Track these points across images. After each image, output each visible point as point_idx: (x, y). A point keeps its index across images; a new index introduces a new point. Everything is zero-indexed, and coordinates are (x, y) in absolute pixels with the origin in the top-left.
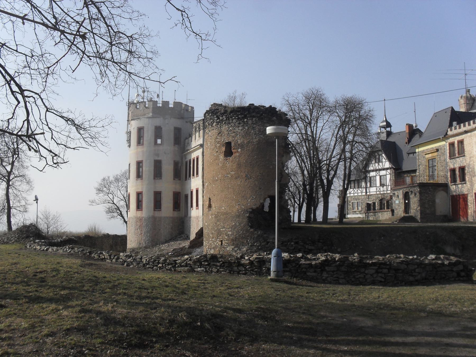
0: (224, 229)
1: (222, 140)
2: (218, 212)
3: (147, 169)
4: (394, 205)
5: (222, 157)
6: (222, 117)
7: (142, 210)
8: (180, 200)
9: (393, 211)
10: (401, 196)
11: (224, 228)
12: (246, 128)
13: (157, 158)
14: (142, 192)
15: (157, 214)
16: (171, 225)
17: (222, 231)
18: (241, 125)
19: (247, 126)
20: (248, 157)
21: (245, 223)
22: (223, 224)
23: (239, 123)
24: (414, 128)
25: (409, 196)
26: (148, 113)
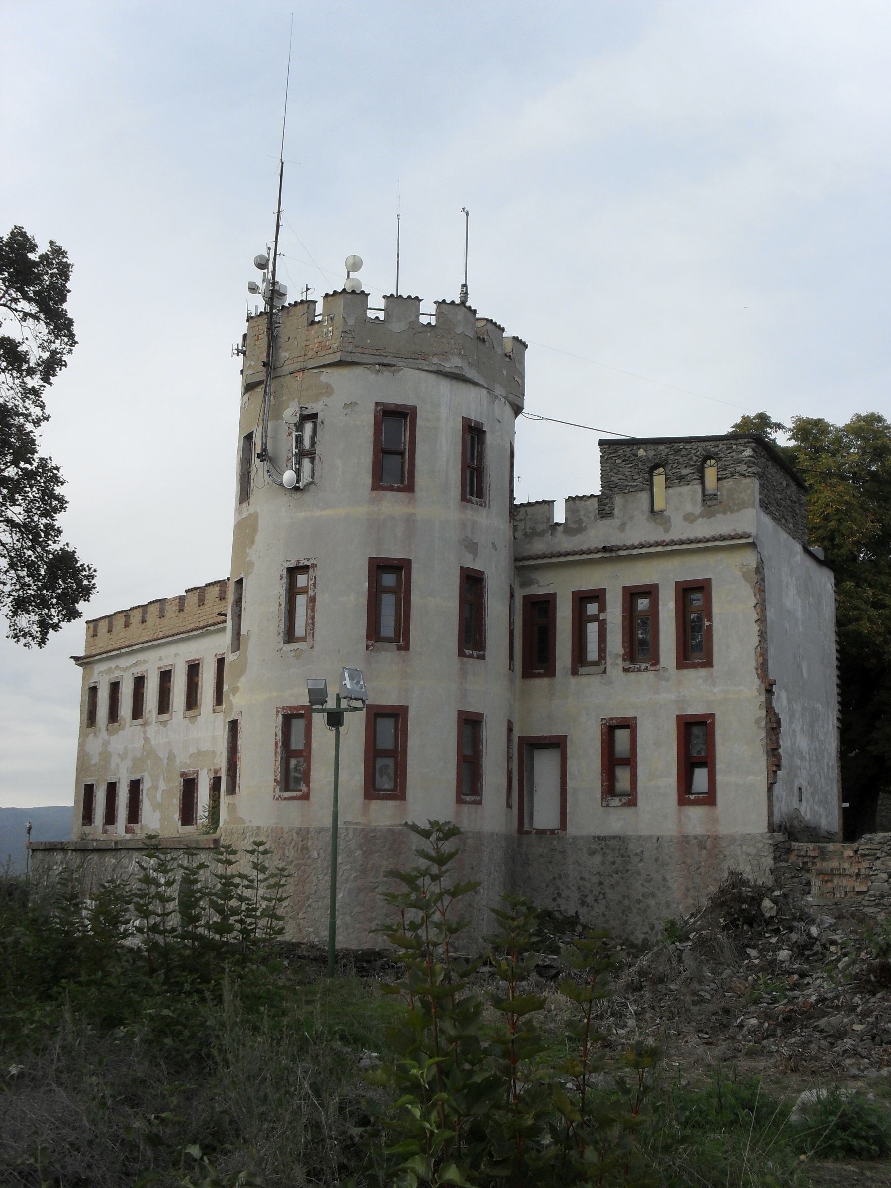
14: (405, 709)
16: (504, 868)
26: (444, 355)
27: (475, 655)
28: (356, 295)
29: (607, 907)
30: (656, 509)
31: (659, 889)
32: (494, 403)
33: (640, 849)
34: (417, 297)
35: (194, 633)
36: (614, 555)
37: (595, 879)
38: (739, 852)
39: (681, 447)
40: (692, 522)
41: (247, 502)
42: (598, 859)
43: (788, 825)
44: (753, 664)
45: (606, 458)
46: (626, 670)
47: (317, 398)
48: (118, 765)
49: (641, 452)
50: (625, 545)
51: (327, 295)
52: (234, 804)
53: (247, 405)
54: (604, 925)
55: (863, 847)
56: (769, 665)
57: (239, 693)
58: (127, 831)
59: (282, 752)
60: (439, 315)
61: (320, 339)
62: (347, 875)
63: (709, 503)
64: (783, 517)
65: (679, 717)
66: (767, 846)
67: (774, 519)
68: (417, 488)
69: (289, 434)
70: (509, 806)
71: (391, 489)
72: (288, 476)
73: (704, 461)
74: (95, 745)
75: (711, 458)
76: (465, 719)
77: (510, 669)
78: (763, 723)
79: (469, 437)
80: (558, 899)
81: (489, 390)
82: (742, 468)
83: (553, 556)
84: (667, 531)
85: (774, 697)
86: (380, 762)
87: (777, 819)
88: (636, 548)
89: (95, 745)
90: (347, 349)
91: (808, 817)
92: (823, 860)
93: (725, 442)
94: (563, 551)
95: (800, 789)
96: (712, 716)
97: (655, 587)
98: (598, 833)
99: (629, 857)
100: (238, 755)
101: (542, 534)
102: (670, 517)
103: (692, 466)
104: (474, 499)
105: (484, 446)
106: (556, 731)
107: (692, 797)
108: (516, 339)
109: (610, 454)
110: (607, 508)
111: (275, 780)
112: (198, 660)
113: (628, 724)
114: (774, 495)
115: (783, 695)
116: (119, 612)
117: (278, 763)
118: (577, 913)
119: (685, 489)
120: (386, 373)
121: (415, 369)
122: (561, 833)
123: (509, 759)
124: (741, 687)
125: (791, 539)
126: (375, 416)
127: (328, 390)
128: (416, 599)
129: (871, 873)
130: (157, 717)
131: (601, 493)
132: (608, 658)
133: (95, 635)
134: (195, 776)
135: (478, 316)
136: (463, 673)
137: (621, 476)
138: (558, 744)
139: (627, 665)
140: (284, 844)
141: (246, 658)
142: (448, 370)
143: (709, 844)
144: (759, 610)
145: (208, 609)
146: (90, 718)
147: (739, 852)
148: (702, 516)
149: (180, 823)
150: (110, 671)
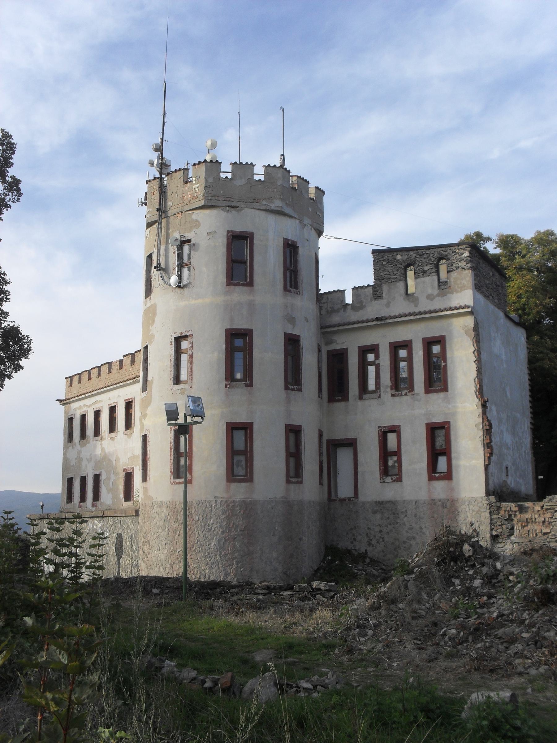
14: (251, 424)
16: (318, 523)
26: (270, 199)
27: (296, 389)
28: (213, 164)
29: (385, 547)
30: (409, 292)
31: (417, 534)
32: (303, 228)
33: (405, 509)
34: (252, 164)
35: (129, 382)
36: (383, 322)
37: (377, 529)
38: (467, 509)
39: (424, 253)
40: (432, 300)
41: (150, 297)
42: (378, 516)
43: (499, 491)
44: (473, 389)
45: (376, 261)
46: (393, 395)
47: (191, 229)
48: (86, 466)
49: (399, 257)
50: (390, 316)
51: (195, 165)
52: (146, 488)
53: (148, 236)
54: (383, 558)
55: (547, 504)
56: (484, 389)
57: (147, 418)
58: (93, 505)
59: (174, 454)
60: (266, 174)
61: (191, 192)
62: (217, 530)
63: (442, 287)
64: (491, 295)
65: (427, 424)
66: (485, 505)
67: (485, 296)
68: (255, 283)
69: (174, 253)
70: (321, 484)
71: (238, 285)
72: (174, 279)
73: (439, 261)
74: (72, 454)
75: (443, 258)
76: (290, 430)
77: (319, 397)
78: (481, 426)
79: (288, 251)
80: (354, 542)
81: (301, 221)
82: (463, 264)
83: (344, 324)
84: (416, 306)
85: (488, 409)
86: (236, 458)
87: (491, 487)
88: (397, 317)
89: (72, 454)
90: (208, 198)
91: (513, 485)
92: (521, 513)
93: (451, 248)
94: (351, 321)
95: (507, 468)
96: (448, 423)
97: (410, 342)
98: (378, 500)
99: (398, 514)
100: (148, 456)
101: (338, 311)
102: (418, 298)
103: (431, 264)
104: (292, 290)
105: (298, 256)
106: (350, 435)
107: (437, 475)
108: (317, 188)
109: (379, 258)
110: (378, 293)
111: (171, 472)
112: (131, 399)
113: (396, 430)
114: (484, 281)
115: (494, 408)
116: (85, 371)
117: (172, 461)
118: (366, 550)
119: (427, 279)
120: (234, 212)
121: (252, 208)
122: (355, 500)
123: (320, 454)
124: (466, 404)
125: (496, 309)
126: (227, 239)
127: (197, 224)
128: (256, 354)
129: (552, 521)
130: (108, 435)
131: (374, 284)
132: (381, 388)
133: (71, 385)
134: (131, 471)
135: (291, 174)
136: (288, 401)
137: (386, 273)
138: (352, 444)
139: (394, 392)
140: (177, 511)
141: (151, 396)
142: (273, 208)
143: (448, 504)
144: (476, 354)
145: (137, 367)
146: (70, 437)
147: (467, 509)
148: (438, 295)
149: (124, 500)
150: (80, 407)
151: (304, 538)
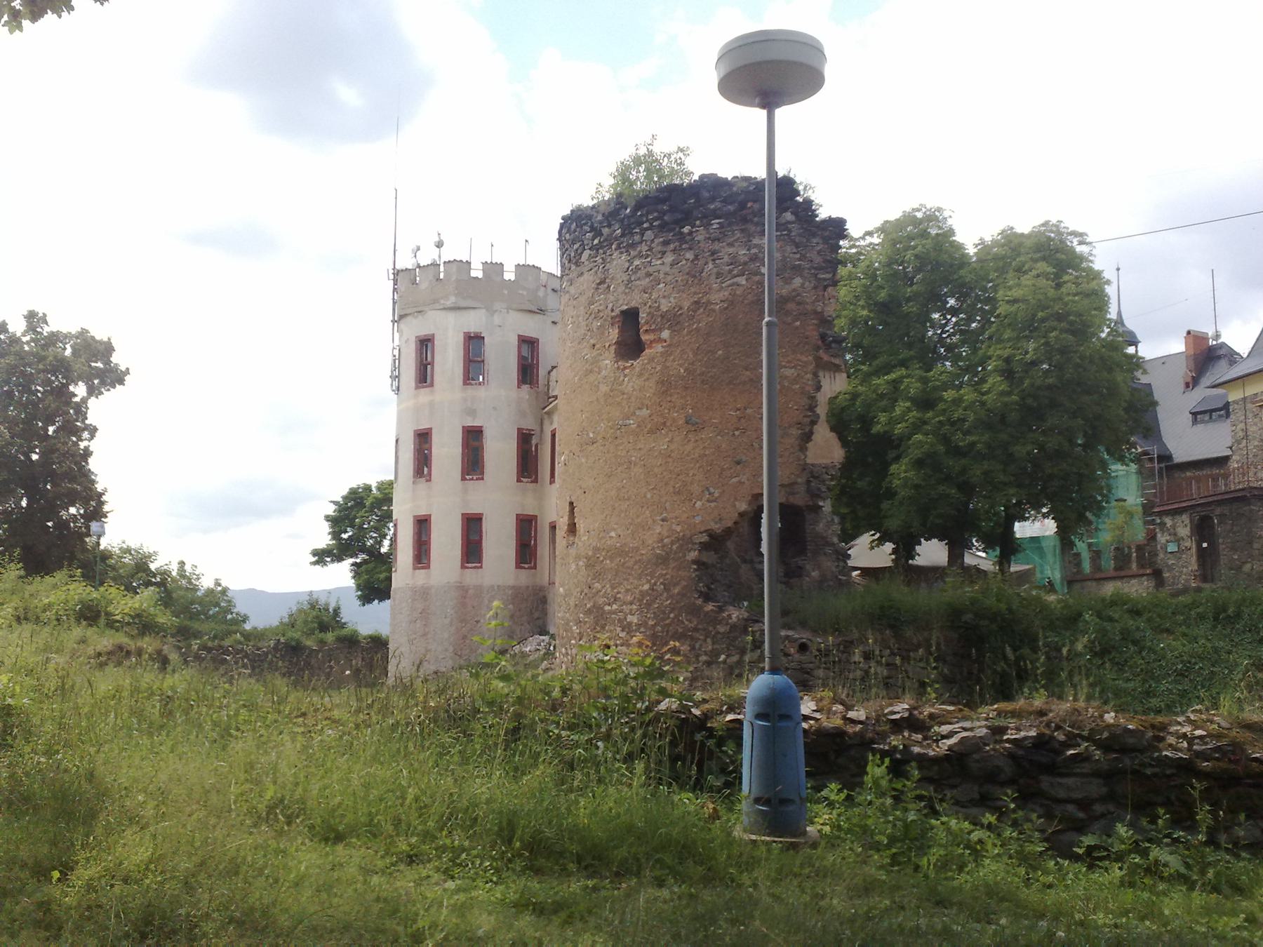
0: (615, 607)
1: (610, 306)
2: (596, 549)
3: (447, 451)
4: (1161, 556)
5: (608, 361)
6: (609, 226)
7: (428, 567)
8: (535, 540)
9: (1157, 574)
10: (1184, 532)
11: (616, 599)
12: (690, 255)
13: (470, 422)
15: (472, 577)
17: (611, 612)
18: (672, 246)
19: (690, 249)
20: (695, 354)
21: (684, 583)
22: (613, 588)
23: (666, 243)
24: (1211, 342)
25: (1212, 527)
32: (492, 315)
151: (482, 621)
